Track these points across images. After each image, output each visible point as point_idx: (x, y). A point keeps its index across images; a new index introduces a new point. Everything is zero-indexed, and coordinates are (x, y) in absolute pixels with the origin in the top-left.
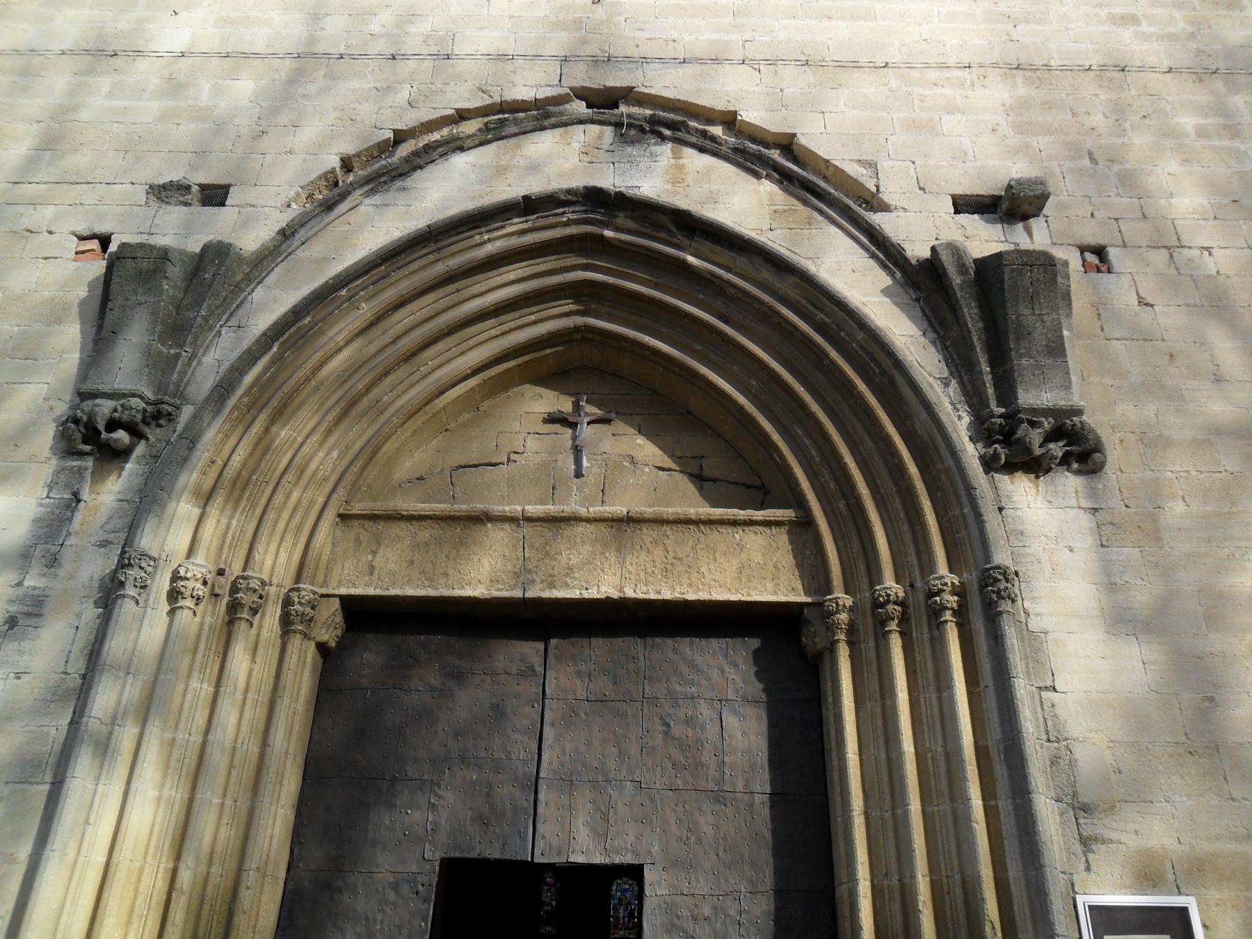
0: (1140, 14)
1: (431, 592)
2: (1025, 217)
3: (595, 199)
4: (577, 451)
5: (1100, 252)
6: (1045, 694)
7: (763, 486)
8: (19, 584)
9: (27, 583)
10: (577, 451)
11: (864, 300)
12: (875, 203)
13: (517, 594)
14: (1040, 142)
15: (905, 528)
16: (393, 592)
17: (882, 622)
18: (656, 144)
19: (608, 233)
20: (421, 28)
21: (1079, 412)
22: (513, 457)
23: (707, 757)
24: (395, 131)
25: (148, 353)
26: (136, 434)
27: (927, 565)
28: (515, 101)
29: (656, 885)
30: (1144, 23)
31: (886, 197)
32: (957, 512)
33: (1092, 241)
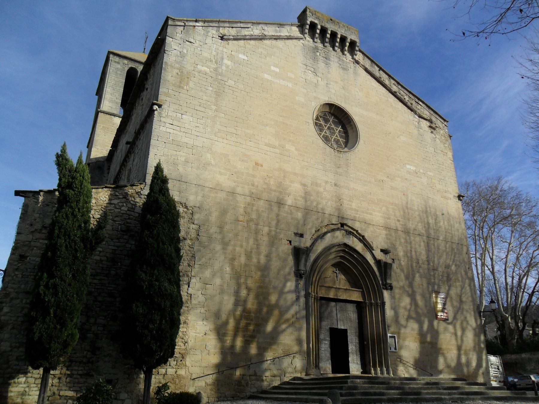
1: (327, 297)
2: (387, 254)
3: (345, 245)
4: (337, 277)
5: (393, 259)
9: (297, 294)
10: (337, 277)
12: (373, 250)
14: (389, 241)
16: (325, 296)
17: (371, 305)
20: (320, 206)
23: (352, 318)
27: (377, 300)
29: (349, 332)
31: (374, 248)
33: (393, 258)
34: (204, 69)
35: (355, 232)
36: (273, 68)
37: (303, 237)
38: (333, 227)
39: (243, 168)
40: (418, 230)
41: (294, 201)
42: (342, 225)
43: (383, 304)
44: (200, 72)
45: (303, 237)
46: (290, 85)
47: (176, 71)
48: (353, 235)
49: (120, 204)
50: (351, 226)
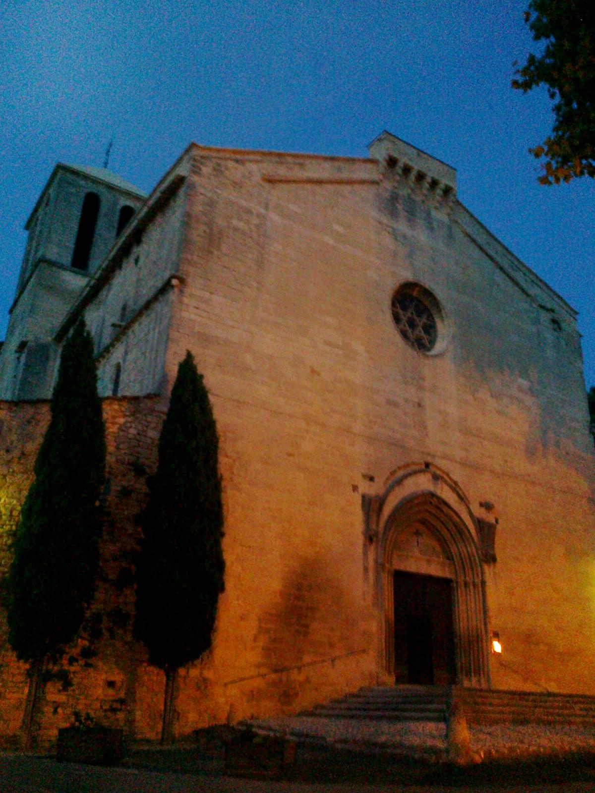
34: (241, 225)
35: (445, 477)
38: (414, 468)
42: (427, 465)
43: (483, 583)
44: (236, 229)
47: (203, 228)
49: (129, 425)
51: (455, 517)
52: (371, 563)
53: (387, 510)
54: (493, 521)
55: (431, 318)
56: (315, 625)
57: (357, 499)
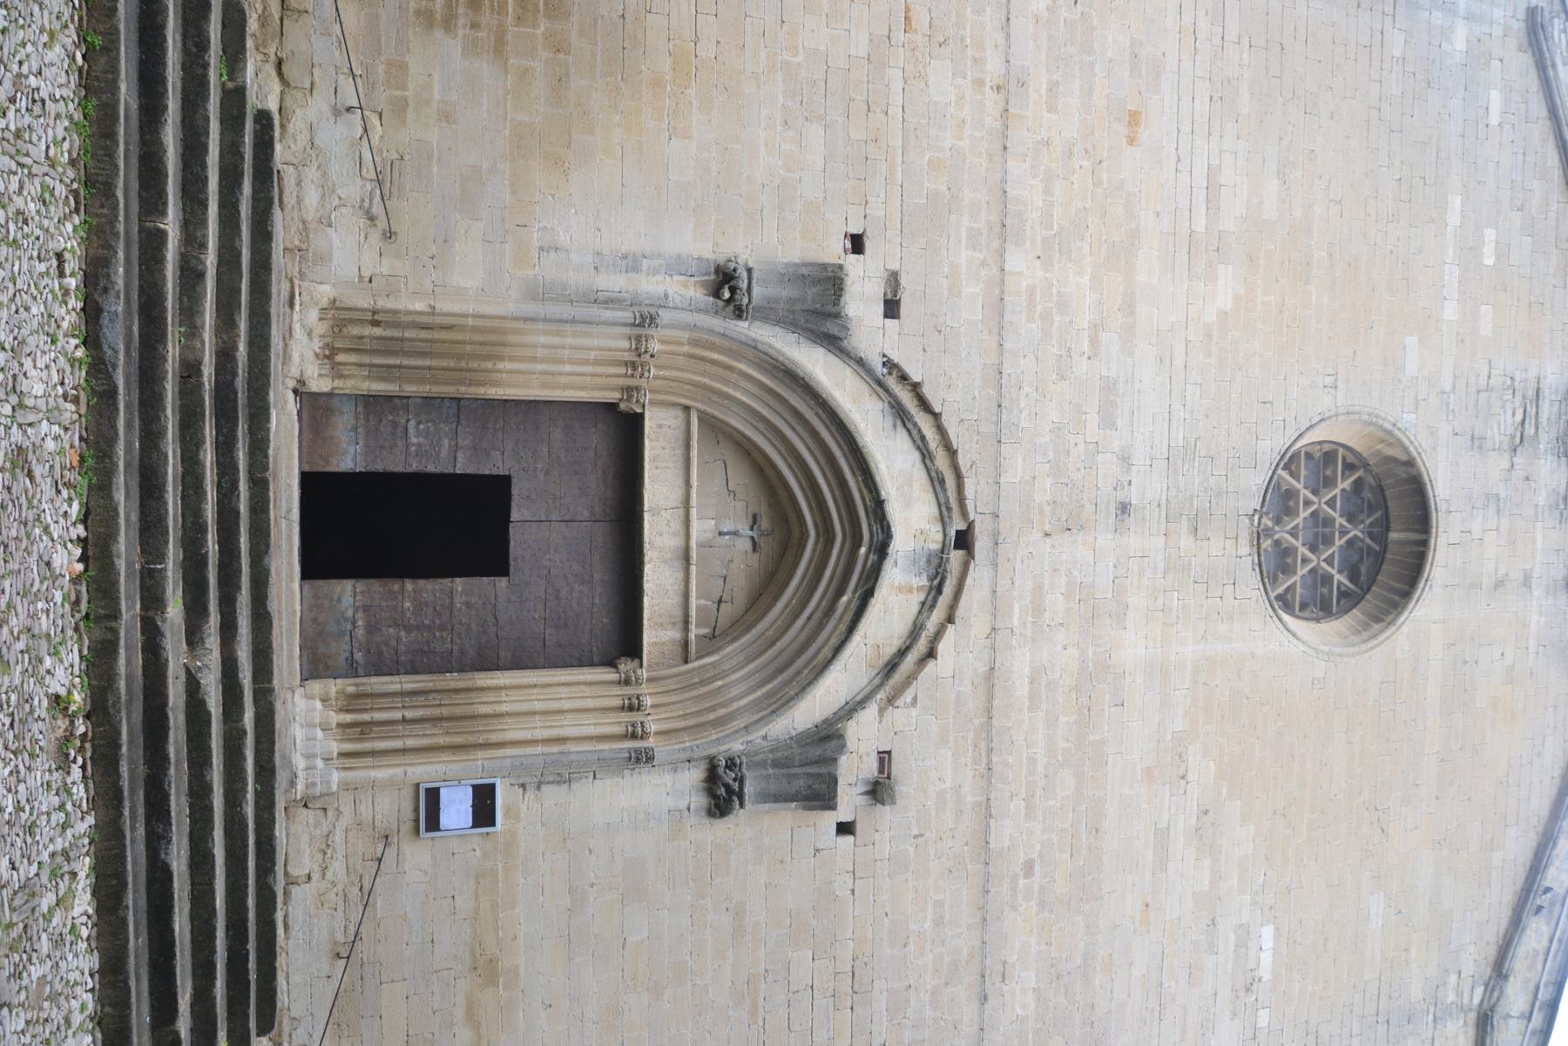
0: (1034, 879)
6: (592, 774)
7: (714, 637)
8: (644, 257)
11: (817, 696)
13: (646, 507)
15: (681, 713)
16: (647, 442)
18: (928, 576)
19: (863, 550)
21: (742, 805)
22: (732, 495)
24: (941, 414)
25: (777, 300)
26: (729, 301)
28: (964, 484)
29: (502, 582)
30: (1025, 881)
32: (687, 739)
36: (1490, 234)
37: (886, 316)
39: (1110, 54)
40: (1006, 988)
41: (1024, 284)
42: (964, 541)
45: (886, 316)
46: (1450, 312)
48: (931, 589)
50: (969, 581)
51: (834, 641)
52: (652, 286)
53: (816, 363)
54: (843, 814)
55: (1349, 600)
56: (452, 47)
57: (833, 250)
